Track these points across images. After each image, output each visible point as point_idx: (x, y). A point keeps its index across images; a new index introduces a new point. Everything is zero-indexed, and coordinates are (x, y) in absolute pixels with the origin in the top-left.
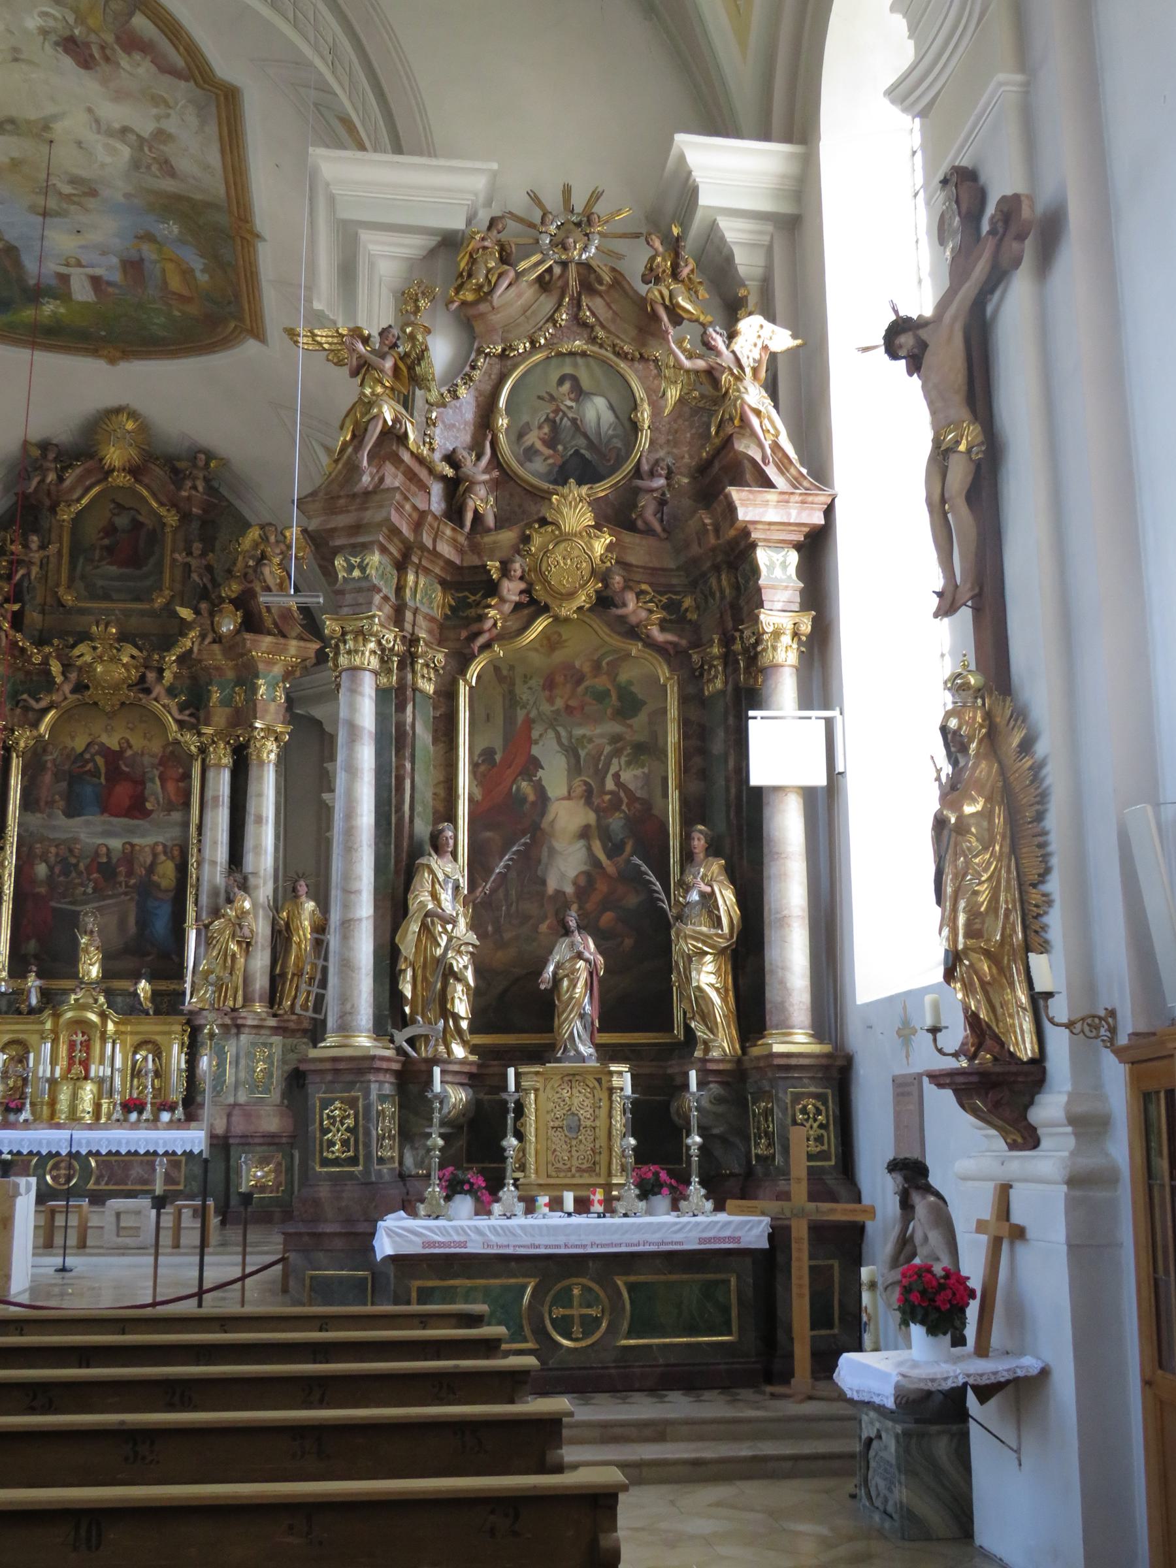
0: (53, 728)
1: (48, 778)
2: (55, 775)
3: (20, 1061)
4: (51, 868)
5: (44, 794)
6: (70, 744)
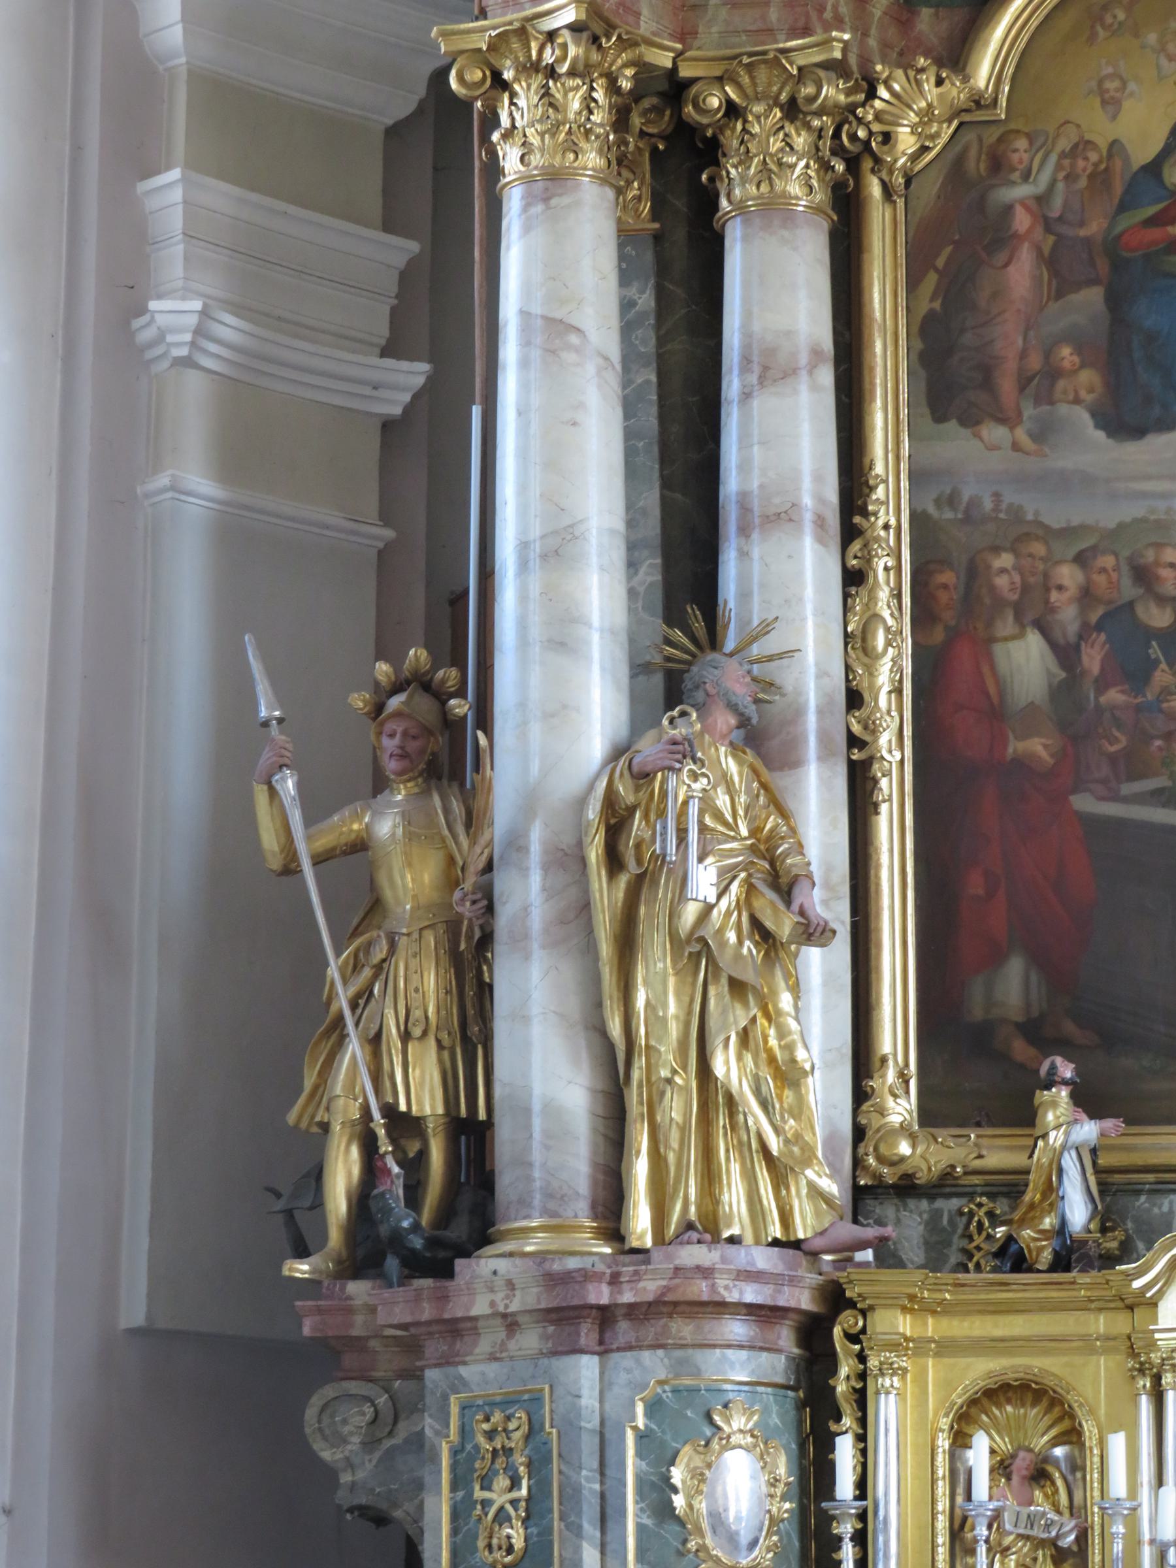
0: (1026, 64)
1: (1021, 274)
2: (1051, 262)
3: (1040, 1475)
4: (1066, 654)
5: (1009, 340)
6: (1102, 130)
